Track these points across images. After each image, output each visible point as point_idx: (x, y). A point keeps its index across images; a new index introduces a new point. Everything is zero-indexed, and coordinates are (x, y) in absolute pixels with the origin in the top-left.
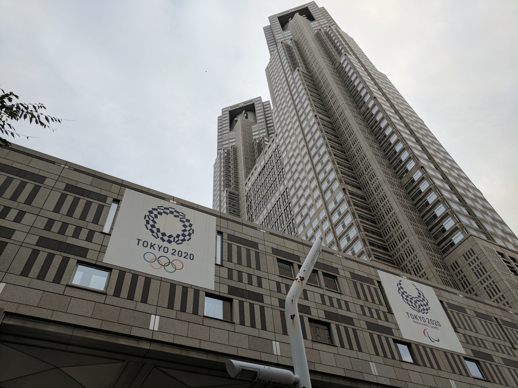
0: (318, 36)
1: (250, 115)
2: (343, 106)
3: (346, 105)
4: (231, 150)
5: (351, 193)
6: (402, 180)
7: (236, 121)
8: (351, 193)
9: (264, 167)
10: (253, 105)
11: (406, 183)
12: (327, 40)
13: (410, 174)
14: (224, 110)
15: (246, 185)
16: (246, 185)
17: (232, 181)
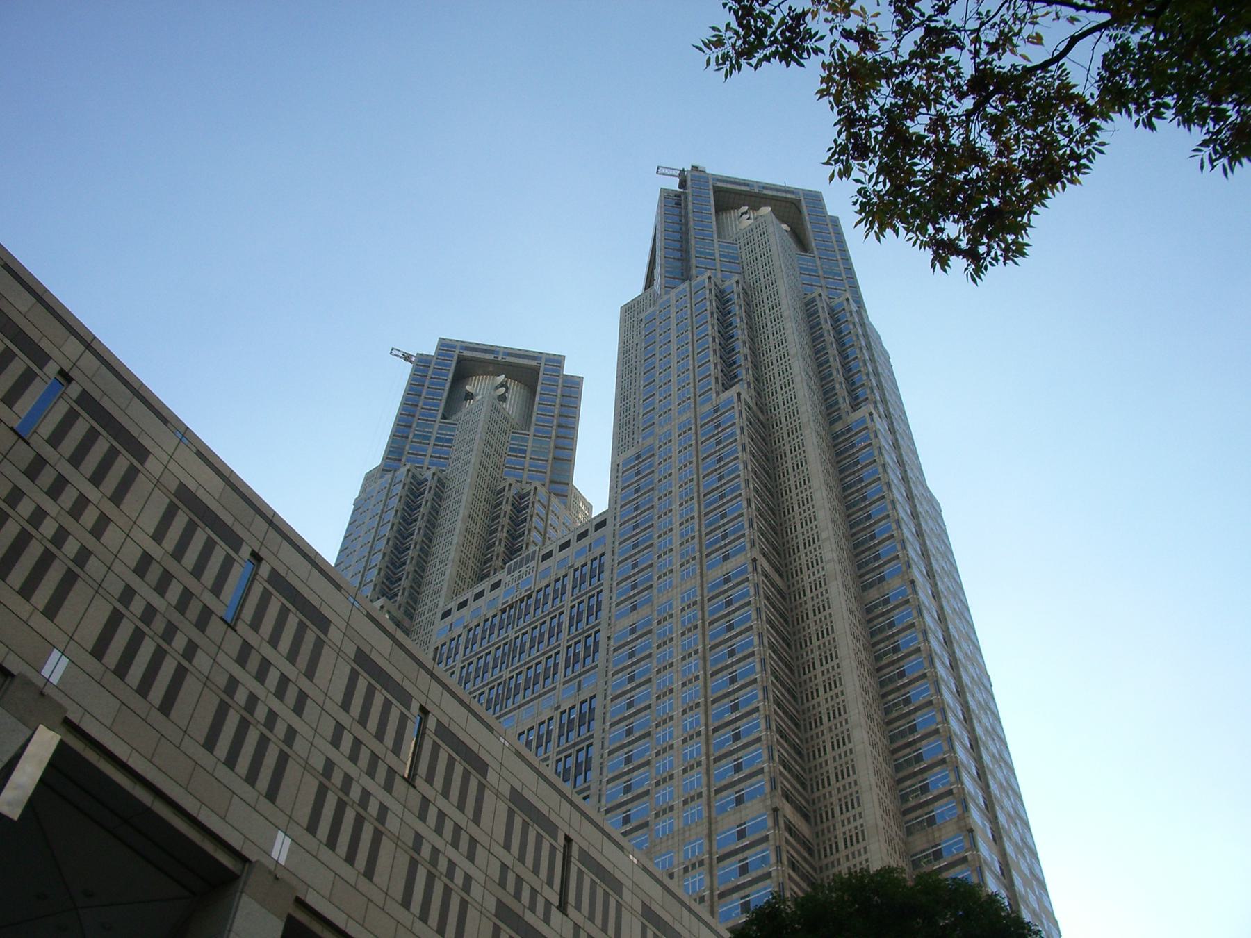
0: (809, 309)
1: (515, 391)
2: (829, 567)
3: (838, 568)
4: (432, 483)
5: (790, 829)
6: (910, 839)
7: (470, 396)
8: (790, 829)
9: (529, 597)
10: (535, 371)
11: (919, 849)
12: (827, 326)
13: (937, 835)
14: (445, 346)
15: (446, 614)
16: (446, 614)
17: (405, 583)
